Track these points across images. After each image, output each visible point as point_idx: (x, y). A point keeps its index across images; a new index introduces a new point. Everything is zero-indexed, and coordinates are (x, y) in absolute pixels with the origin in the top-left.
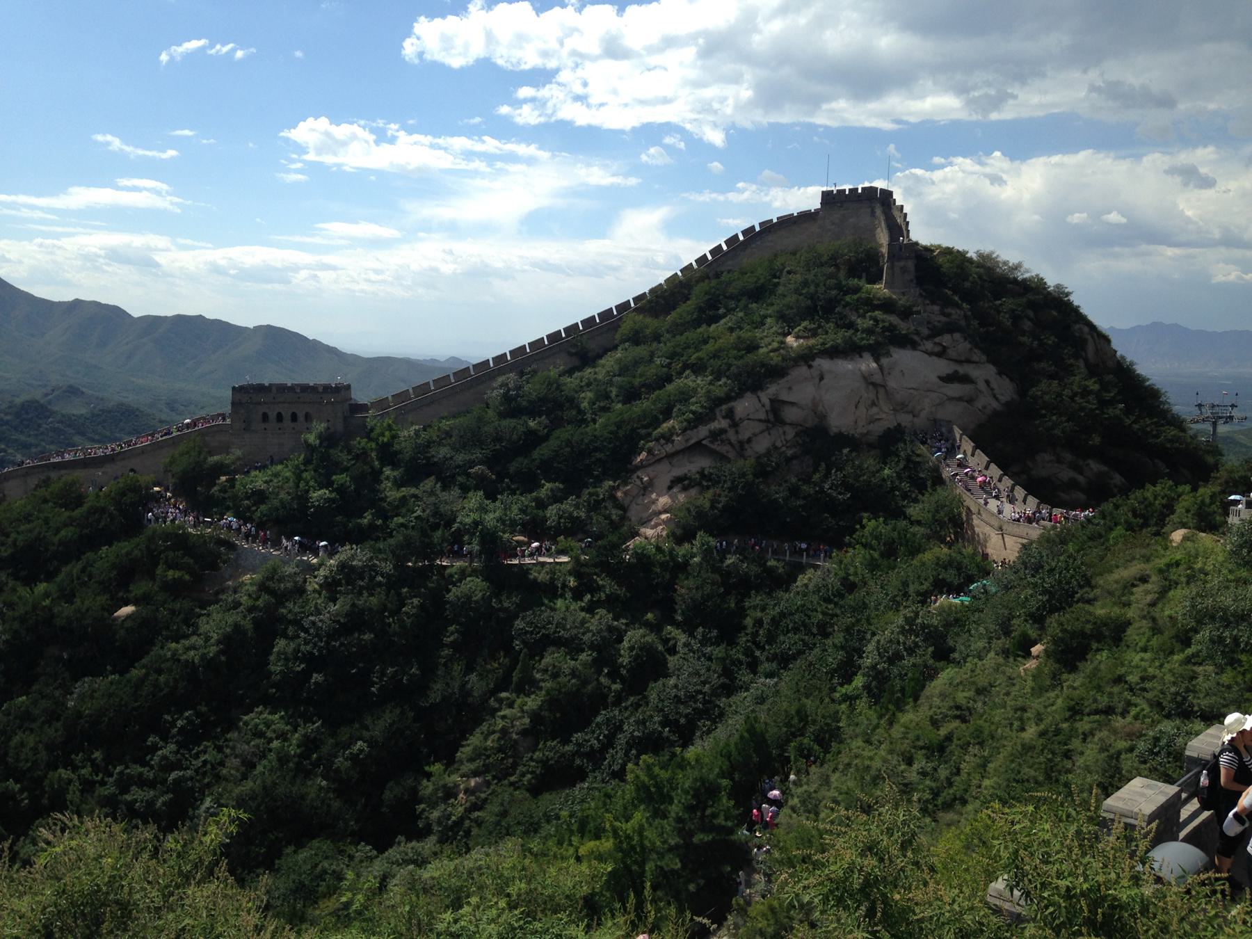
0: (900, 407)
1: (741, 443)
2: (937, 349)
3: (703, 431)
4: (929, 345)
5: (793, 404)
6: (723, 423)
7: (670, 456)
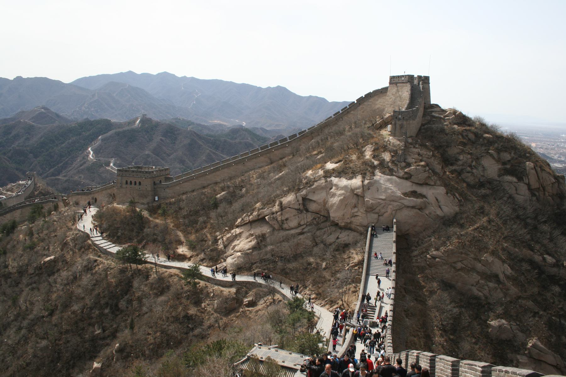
0: (370, 209)
2: (406, 176)
5: (315, 201)
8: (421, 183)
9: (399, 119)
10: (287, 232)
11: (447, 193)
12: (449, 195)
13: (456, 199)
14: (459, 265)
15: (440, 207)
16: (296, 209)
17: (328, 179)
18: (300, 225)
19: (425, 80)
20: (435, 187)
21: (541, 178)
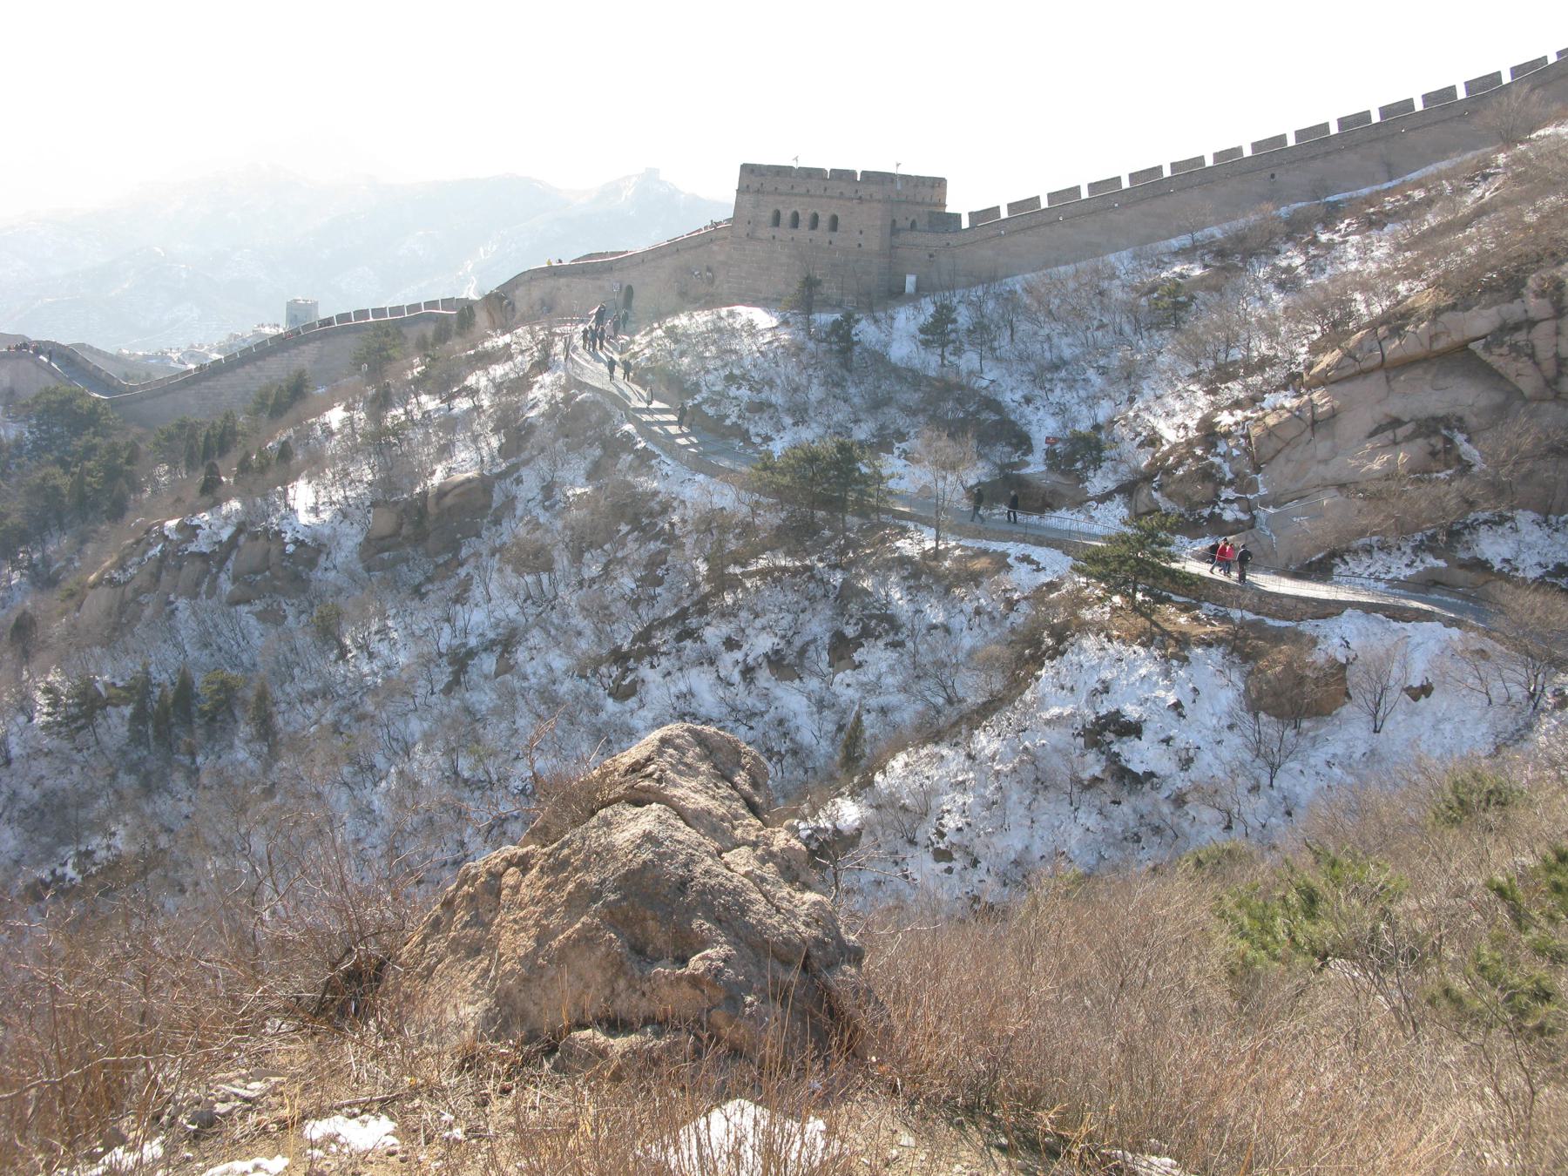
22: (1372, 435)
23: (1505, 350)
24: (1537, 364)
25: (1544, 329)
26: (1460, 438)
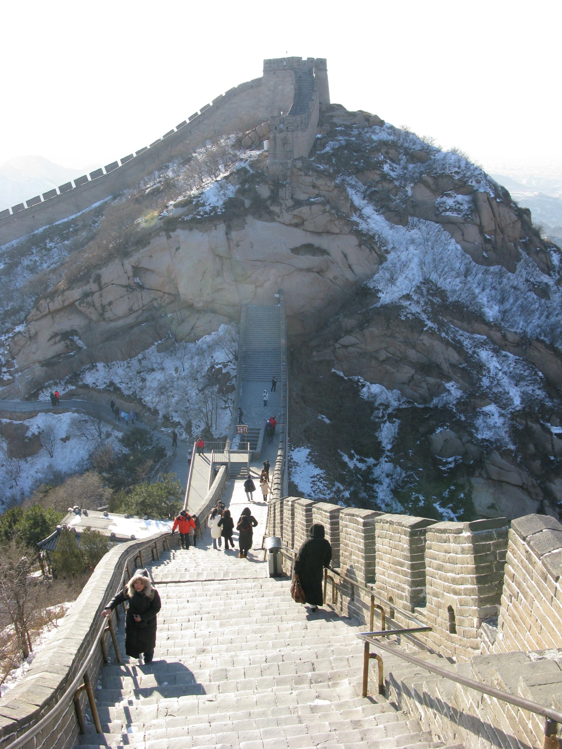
1: (103, 307)
2: (295, 221)
3: (76, 294)
4: (287, 217)
6: (93, 286)
7: (53, 313)
8: (320, 231)
9: (281, 131)
10: (112, 324)
11: (360, 245)
12: (363, 247)
13: (373, 253)
14: (383, 355)
15: (350, 267)
16: (123, 286)
17: (171, 234)
18: (131, 311)
19: (320, 65)
20: (341, 236)
21: (497, 215)
22: (49, 340)
23: (85, 305)
24: (96, 309)
25: (97, 295)
26: (76, 338)
